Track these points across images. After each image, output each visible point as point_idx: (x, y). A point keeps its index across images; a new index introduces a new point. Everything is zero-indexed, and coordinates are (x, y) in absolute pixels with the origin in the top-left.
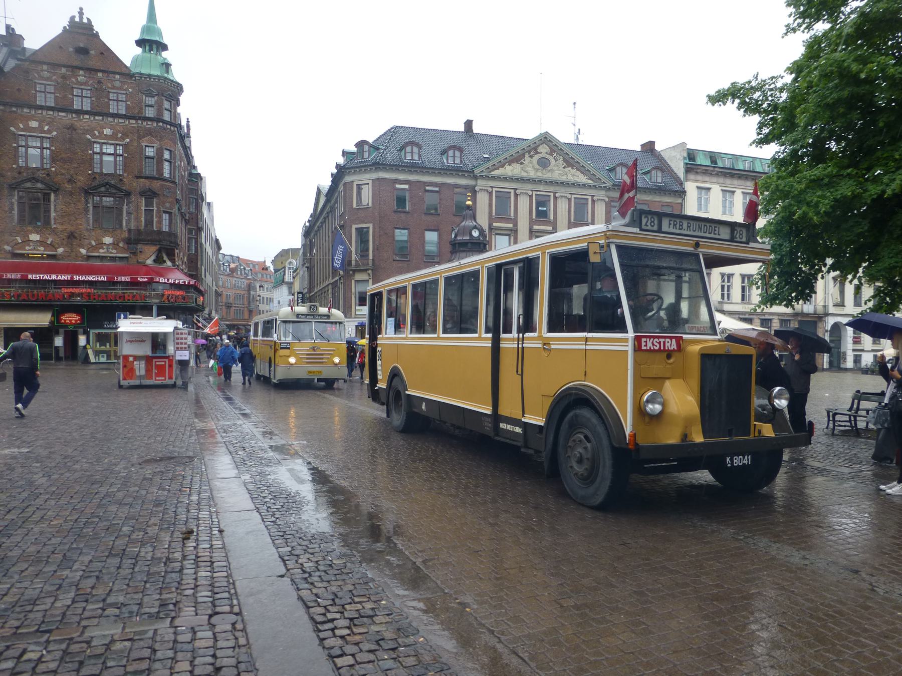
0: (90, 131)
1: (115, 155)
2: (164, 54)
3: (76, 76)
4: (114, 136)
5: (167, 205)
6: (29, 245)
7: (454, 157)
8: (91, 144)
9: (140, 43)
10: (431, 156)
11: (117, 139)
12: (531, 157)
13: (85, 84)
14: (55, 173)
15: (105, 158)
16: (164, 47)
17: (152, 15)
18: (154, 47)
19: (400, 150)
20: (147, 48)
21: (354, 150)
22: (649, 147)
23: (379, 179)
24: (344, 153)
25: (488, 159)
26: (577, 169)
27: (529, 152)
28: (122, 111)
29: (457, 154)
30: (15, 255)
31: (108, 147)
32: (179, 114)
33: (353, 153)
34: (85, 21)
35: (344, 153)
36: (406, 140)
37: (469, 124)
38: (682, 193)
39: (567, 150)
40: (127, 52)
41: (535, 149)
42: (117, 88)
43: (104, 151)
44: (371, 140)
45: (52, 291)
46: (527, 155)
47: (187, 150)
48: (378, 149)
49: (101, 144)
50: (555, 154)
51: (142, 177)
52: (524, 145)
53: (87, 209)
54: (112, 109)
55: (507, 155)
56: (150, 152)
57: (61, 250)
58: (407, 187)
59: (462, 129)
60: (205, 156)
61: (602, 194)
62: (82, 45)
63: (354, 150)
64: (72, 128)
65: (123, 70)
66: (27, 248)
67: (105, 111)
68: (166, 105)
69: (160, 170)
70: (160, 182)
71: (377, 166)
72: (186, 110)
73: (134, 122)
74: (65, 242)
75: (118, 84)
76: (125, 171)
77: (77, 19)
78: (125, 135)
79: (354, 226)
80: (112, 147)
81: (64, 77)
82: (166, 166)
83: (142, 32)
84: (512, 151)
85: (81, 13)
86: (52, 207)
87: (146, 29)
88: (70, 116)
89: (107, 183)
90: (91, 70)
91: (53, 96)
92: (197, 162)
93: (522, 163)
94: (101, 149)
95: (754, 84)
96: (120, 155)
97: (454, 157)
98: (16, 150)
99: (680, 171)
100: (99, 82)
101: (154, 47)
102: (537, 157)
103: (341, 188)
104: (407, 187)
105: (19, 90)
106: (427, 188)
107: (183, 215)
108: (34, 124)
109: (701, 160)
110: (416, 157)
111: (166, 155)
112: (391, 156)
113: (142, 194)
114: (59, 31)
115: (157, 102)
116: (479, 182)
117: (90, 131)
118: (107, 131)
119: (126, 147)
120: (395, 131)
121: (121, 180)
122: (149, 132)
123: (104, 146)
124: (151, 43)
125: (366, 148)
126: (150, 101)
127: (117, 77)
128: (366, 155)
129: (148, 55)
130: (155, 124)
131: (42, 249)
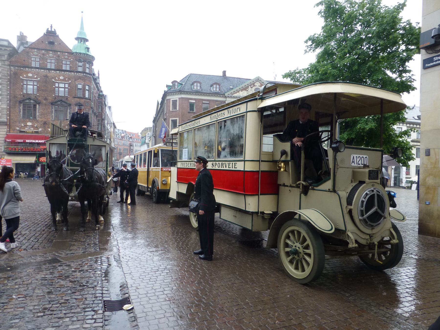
0: (54, 78)
1: (65, 88)
2: (87, 43)
3: (49, 54)
4: (64, 80)
5: (87, 110)
6: (27, 127)
7: (216, 88)
8: (54, 83)
9: (77, 39)
10: (206, 88)
11: (66, 81)
12: (252, 88)
13: (53, 57)
14: (39, 96)
15: (60, 89)
16: (87, 40)
17: (82, 27)
18: (83, 40)
19: (192, 85)
20: (80, 41)
21: (171, 85)
23: (182, 98)
24: (167, 86)
25: (232, 89)
27: (251, 85)
28: (68, 69)
30: (21, 132)
31: (62, 84)
32: (93, 69)
33: (171, 86)
34: (53, 30)
35: (167, 86)
36: (195, 80)
37: (224, 72)
40: (71, 43)
41: (254, 84)
42: (66, 59)
43: (60, 86)
44: (178, 81)
45: (36, 147)
46: (250, 87)
47: (97, 84)
48: (182, 84)
49: (59, 83)
51: (76, 98)
52: (248, 82)
53: (52, 111)
54: (64, 68)
55: (241, 87)
56: (80, 86)
57: (40, 129)
58: (194, 101)
60: (106, 87)
62: (51, 41)
63: (171, 85)
64: (46, 76)
65: (69, 51)
66: (26, 128)
67: (60, 69)
68: (87, 66)
69: (84, 94)
70: (84, 100)
71: (181, 92)
72: (96, 67)
73: (73, 73)
74: (42, 126)
75: (66, 57)
76: (69, 95)
77: (50, 30)
78: (69, 79)
79: (171, 119)
80: (63, 84)
81: (43, 54)
82: (87, 92)
83: (78, 34)
84: (243, 85)
85: (51, 27)
86: (37, 111)
87: (80, 33)
88: (45, 71)
89: (61, 100)
90: (55, 51)
91: (38, 63)
92: (102, 89)
93: (247, 91)
94: (59, 85)
95: (297, 71)
96: (67, 88)
97: (216, 88)
98: (23, 86)
100: (59, 56)
101: (83, 40)
102: (254, 88)
103: (166, 102)
104: (194, 101)
105: (24, 60)
106: (204, 102)
107: (95, 114)
108: (30, 75)
110: (199, 88)
111: (87, 88)
113: (76, 105)
114: (42, 35)
115: (83, 65)
116: (227, 99)
117: (54, 78)
118: (61, 78)
119: (69, 84)
120: (190, 76)
121: (67, 99)
122: (80, 78)
123: (60, 84)
124: (82, 40)
125: (176, 84)
126: (80, 64)
127: (66, 54)
128: (176, 87)
129: (80, 44)
130: (82, 74)
131: (32, 129)
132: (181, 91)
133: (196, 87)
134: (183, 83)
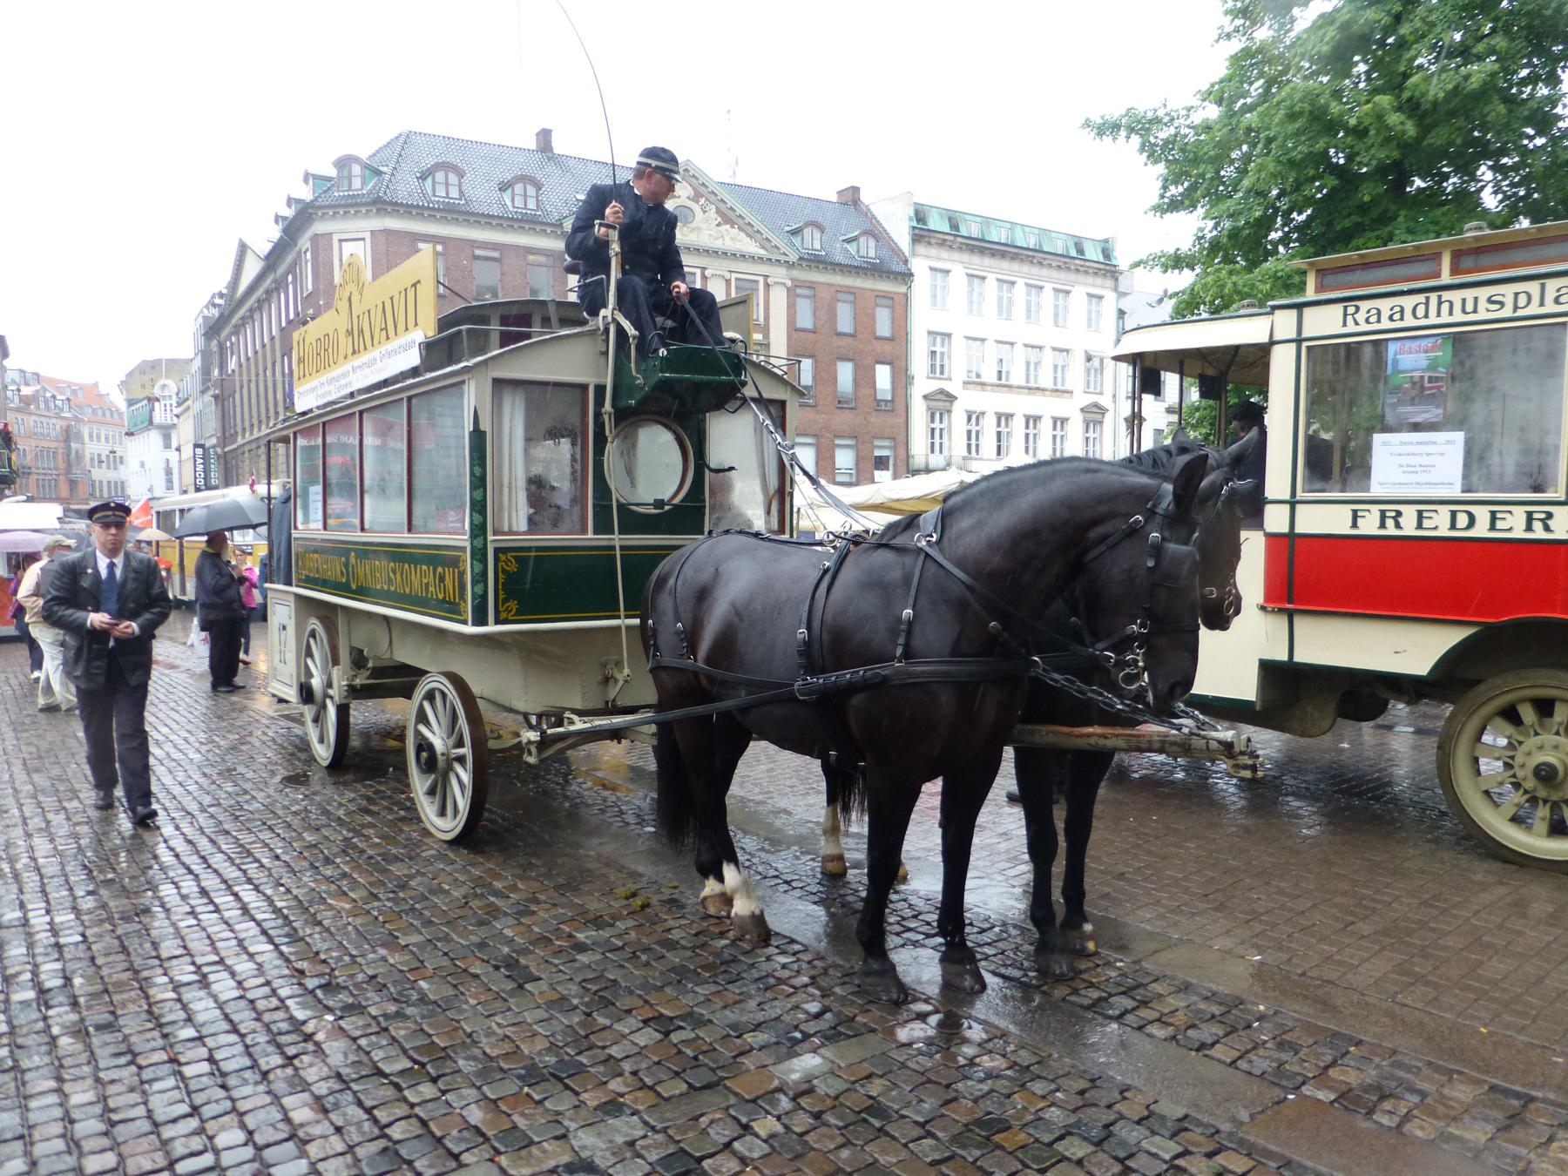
10: (482, 194)
19: (423, 178)
21: (333, 173)
22: (851, 198)
23: (387, 232)
26: (740, 229)
29: (531, 191)
33: (329, 179)
37: (545, 136)
38: (907, 277)
39: (723, 193)
48: (379, 173)
50: (702, 201)
59: (532, 144)
61: (780, 274)
63: (333, 173)
71: (381, 205)
99: (903, 239)
103: (304, 243)
106: (478, 252)
109: (937, 223)
112: (406, 188)
120: (405, 141)
125: (356, 169)
128: (357, 183)
132: (385, 202)
133: (442, 190)
134: (384, 169)
